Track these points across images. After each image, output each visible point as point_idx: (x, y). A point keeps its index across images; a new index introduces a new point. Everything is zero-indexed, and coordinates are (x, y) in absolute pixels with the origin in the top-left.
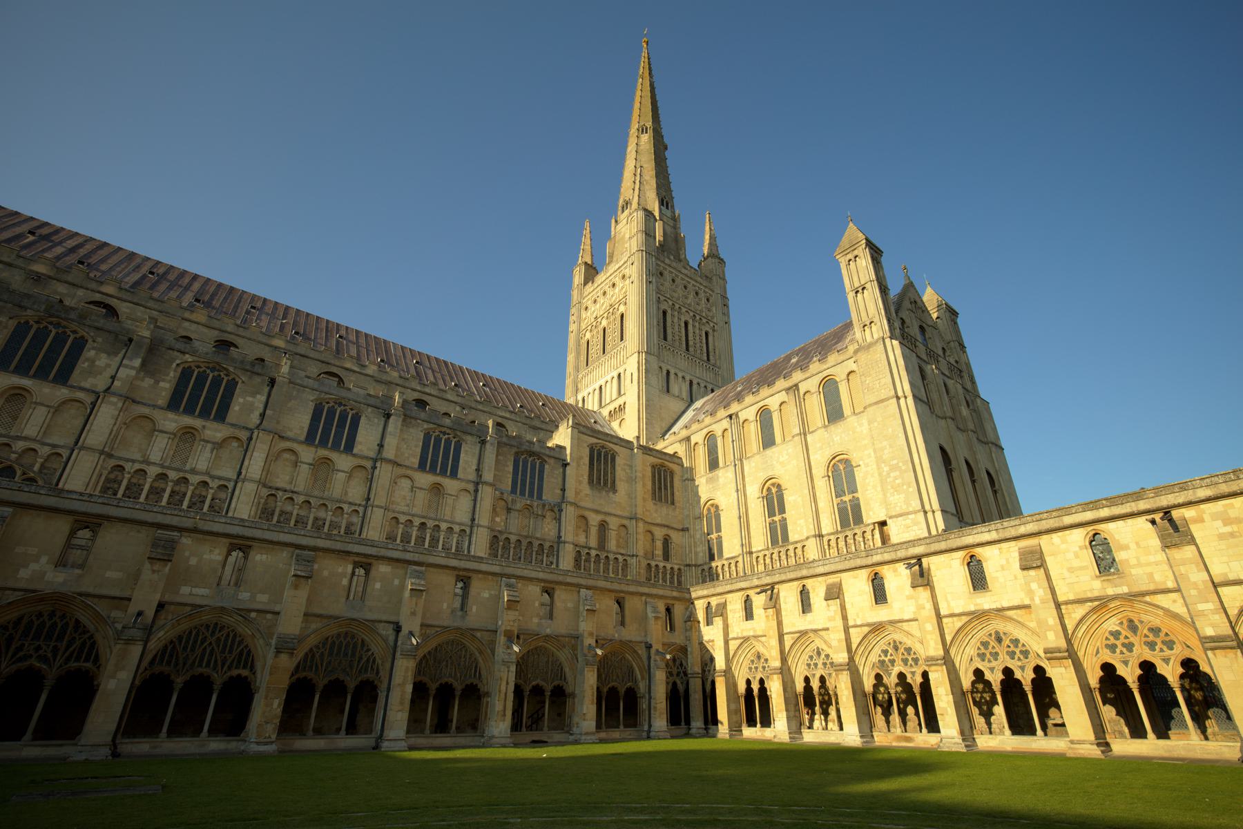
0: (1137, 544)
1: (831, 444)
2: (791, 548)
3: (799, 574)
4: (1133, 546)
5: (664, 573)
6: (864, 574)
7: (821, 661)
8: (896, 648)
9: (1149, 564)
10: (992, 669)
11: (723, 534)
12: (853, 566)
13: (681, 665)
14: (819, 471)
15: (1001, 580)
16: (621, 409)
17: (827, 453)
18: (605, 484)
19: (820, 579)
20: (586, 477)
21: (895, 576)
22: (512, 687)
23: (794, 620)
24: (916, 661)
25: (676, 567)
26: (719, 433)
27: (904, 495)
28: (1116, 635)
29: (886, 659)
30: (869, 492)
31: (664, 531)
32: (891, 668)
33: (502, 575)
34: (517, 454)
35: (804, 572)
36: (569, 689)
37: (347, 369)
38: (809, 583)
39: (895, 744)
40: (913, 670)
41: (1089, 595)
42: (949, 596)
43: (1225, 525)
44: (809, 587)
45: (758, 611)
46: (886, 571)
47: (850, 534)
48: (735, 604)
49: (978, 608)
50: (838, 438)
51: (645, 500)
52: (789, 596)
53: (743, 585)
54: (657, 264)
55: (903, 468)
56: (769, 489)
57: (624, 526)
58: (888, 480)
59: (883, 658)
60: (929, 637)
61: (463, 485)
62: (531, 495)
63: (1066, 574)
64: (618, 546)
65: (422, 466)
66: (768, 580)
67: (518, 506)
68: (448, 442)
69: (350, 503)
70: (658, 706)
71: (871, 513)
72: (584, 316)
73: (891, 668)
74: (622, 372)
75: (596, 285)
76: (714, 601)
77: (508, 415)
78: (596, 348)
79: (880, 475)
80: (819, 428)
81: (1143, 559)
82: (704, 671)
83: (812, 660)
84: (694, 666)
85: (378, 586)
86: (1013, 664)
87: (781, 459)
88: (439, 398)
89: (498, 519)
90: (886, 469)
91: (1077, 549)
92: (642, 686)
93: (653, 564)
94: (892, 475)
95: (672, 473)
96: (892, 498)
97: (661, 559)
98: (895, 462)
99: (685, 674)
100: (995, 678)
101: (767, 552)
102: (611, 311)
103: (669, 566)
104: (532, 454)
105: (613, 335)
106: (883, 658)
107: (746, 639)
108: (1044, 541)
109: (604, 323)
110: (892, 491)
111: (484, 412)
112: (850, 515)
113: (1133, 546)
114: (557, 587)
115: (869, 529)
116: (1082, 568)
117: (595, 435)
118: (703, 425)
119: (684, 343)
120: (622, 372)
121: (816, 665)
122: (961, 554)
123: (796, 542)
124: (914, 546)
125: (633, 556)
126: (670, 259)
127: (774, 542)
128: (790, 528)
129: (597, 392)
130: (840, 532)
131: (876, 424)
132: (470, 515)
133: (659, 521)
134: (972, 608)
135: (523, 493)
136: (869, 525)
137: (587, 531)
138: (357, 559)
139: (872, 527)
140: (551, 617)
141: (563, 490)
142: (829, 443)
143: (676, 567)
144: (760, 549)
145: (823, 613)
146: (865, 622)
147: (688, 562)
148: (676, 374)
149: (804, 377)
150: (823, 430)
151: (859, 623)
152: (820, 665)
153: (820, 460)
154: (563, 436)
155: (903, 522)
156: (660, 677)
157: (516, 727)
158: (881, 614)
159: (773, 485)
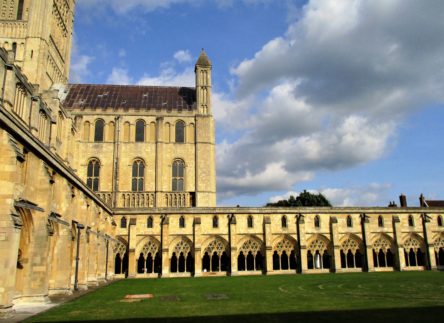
0: (292, 221)
1: (176, 152)
2: (145, 194)
3: (181, 212)
4: (291, 221)
6: (211, 216)
7: (183, 247)
9: (293, 226)
10: (246, 251)
15: (257, 225)
17: (173, 155)
19: (191, 215)
21: (223, 219)
27: (205, 184)
28: (279, 243)
29: (211, 247)
30: (190, 178)
32: (212, 250)
35: (184, 211)
39: (209, 276)
40: (220, 251)
41: (279, 233)
42: (240, 228)
43: (310, 220)
46: (220, 216)
48: (142, 220)
49: (248, 233)
50: (180, 150)
52: (174, 220)
55: (207, 173)
59: (210, 246)
60: (233, 241)
63: (275, 226)
71: (188, 188)
73: (212, 250)
76: (128, 217)
81: (292, 225)
83: (178, 246)
86: (253, 250)
87: (147, 150)
91: (279, 220)
94: (202, 175)
98: (205, 170)
100: (246, 254)
101: (129, 194)
106: (210, 246)
107: (150, 236)
108: (271, 216)
110: (201, 181)
113: (291, 221)
116: (278, 225)
118: (94, 113)
121: (180, 248)
122: (247, 215)
123: (148, 192)
124: (232, 209)
127: (134, 189)
130: (173, 192)
131: (200, 152)
134: (247, 233)
136: (186, 192)
142: (174, 152)
144: (126, 191)
146: (208, 234)
150: (173, 144)
151: (205, 233)
158: (216, 231)
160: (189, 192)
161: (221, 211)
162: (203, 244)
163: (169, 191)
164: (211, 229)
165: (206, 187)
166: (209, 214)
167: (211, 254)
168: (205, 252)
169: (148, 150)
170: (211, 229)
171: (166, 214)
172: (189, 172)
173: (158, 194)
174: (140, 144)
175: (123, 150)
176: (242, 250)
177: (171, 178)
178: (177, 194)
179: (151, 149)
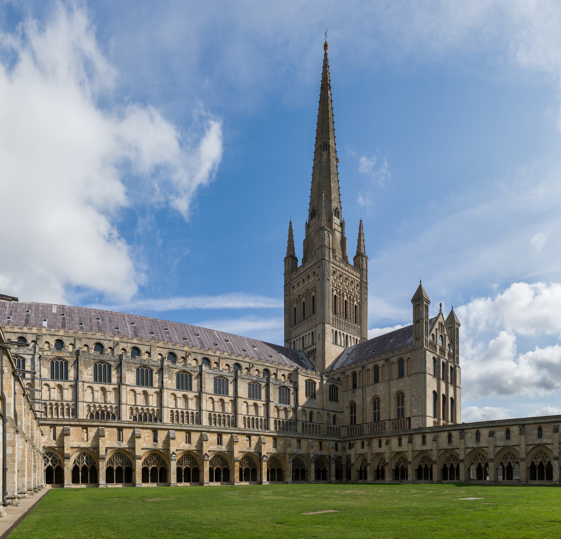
5: (333, 430)
8: (402, 459)
10: (423, 465)
11: (357, 414)
13: (340, 462)
14: (393, 396)
16: (314, 351)
19: (385, 438)
20: (304, 394)
22: (291, 469)
23: (376, 450)
24: (407, 462)
25: (338, 427)
26: (358, 373)
31: (334, 413)
33: (285, 437)
34: (280, 388)
35: (381, 435)
36: (306, 469)
38: (382, 439)
44: (382, 440)
45: (366, 446)
47: (399, 421)
48: (359, 444)
51: (326, 401)
52: (375, 443)
53: (361, 437)
56: (375, 400)
57: (319, 412)
64: (317, 420)
66: (369, 437)
67: (282, 408)
70: (333, 474)
72: (292, 293)
74: (314, 331)
76: (352, 442)
78: (299, 315)
79: (411, 401)
82: (347, 464)
84: (344, 462)
87: (380, 389)
89: (275, 414)
90: (413, 399)
92: (327, 469)
93: (330, 426)
95: (337, 388)
97: (333, 424)
99: (341, 464)
100: (423, 467)
101: (372, 424)
103: (335, 427)
104: (285, 387)
105: (309, 309)
107: (361, 455)
109: (304, 300)
112: (401, 412)
114: (301, 439)
115: (405, 420)
117: (308, 376)
120: (314, 331)
121: (381, 462)
123: (382, 421)
125: (322, 424)
127: (375, 420)
128: (381, 415)
129: (301, 340)
130: (397, 419)
133: (332, 409)
137: (306, 415)
139: (406, 419)
140: (300, 448)
143: (338, 427)
144: (369, 422)
145: (384, 449)
147: (343, 425)
148: (340, 333)
151: (394, 451)
152: (382, 462)
153: (394, 390)
156: (333, 466)
157: (293, 480)
158: (400, 450)
159: (377, 398)
160: (407, 418)
161: (404, 433)
162: (393, 459)
163: (394, 419)
165: (417, 412)
166: (396, 436)
167: (400, 467)
168: (396, 465)
171: (371, 438)
172: (407, 401)
173: (387, 422)
174: (376, 385)
175: (367, 392)
178: (399, 421)
179: (383, 387)
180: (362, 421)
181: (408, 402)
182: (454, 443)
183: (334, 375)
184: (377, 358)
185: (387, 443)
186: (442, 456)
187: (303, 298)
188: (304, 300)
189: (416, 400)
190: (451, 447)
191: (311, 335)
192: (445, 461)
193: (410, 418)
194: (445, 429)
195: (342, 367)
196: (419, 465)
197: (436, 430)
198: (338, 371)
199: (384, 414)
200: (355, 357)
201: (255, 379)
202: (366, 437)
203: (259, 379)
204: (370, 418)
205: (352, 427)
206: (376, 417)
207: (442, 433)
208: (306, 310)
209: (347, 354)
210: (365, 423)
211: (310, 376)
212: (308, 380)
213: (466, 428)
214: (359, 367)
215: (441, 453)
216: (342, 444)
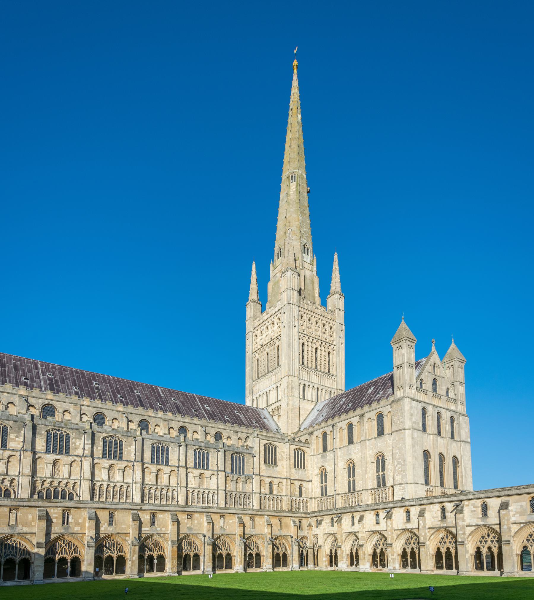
6: (373, 512)
10: (408, 548)
12: (370, 509)
18: (272, 463)
34: (232, 454)
37: (150, 416)
54: (299, 311)
58: (396, 468)
61: (212, 472)
62: (240, 473)
65: (195, 466)
68: (204, 453)
69: (172, 487)
75: (261, 321)
77: (223, 427)
78: (263, 369)
80: (372, 438)
85: (196, 522)
87: (355, 451)
88: (191, 424)
96: (396, 477)
102: (272, 342)
104: (238, 453)
109: (267, 350)
110: (397, 473)
111: (212, 427)
117: (267, 439)
119: (315, 364)
126: (307, 304)
132: (216, 486)
135: (236, 473)
136: (388, 486)
138: (188, 513)
141: (253, 469)
149: (369, 410)
154: (252, 441)
155: (399, 488)
158: (377, 528)
161: (381, 507)
164: (374, 525)
165: (402, 479)
166: (372, 510)
169: (356, 451)
170: (374, 525)
172: (388, 465)
176: (406, 547)
177: (376, 474)
180: (333, 491)
181: (390, 467)
182: (449, 520)
183: (302, 436)
184: (351, 414)
185: (361, 519)
186: (433, 536)
187: (267, 348)
188: (267, 350)
189: (399, 463)
190: (445, 525)
191: (275, 391)
192: (439, 544)
193: (393, 487)
194: (436, 501)
195: (311, 426)
196: (402, 548)
197: (423, 502)
198: (305, 431)
199: (360, 482)
200: (326, 414)
201: (203, 444)
202: (335, 512)
203: (208, 444)
204: (343, 488)
205: (322, 498)
206: (352, 488)
207: (431, 506)
208: (270, 361)
209: (318, 411)
210: (337, 494)
211: (270, 440)
212: (267, 444)
213: (465, 498)
214: (329, 425)
215: (432, 532)
216: (308, 521)
